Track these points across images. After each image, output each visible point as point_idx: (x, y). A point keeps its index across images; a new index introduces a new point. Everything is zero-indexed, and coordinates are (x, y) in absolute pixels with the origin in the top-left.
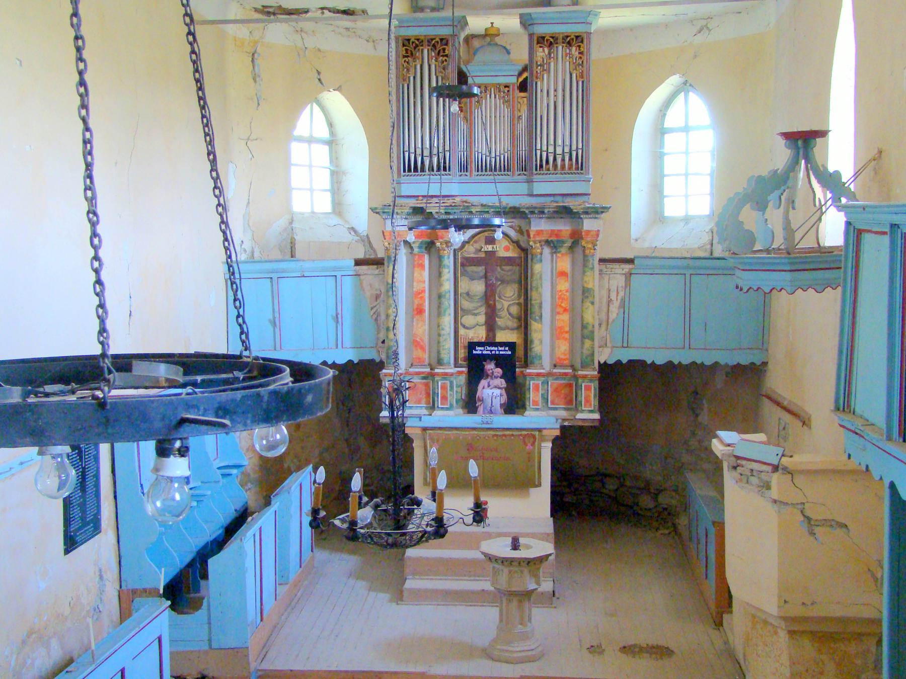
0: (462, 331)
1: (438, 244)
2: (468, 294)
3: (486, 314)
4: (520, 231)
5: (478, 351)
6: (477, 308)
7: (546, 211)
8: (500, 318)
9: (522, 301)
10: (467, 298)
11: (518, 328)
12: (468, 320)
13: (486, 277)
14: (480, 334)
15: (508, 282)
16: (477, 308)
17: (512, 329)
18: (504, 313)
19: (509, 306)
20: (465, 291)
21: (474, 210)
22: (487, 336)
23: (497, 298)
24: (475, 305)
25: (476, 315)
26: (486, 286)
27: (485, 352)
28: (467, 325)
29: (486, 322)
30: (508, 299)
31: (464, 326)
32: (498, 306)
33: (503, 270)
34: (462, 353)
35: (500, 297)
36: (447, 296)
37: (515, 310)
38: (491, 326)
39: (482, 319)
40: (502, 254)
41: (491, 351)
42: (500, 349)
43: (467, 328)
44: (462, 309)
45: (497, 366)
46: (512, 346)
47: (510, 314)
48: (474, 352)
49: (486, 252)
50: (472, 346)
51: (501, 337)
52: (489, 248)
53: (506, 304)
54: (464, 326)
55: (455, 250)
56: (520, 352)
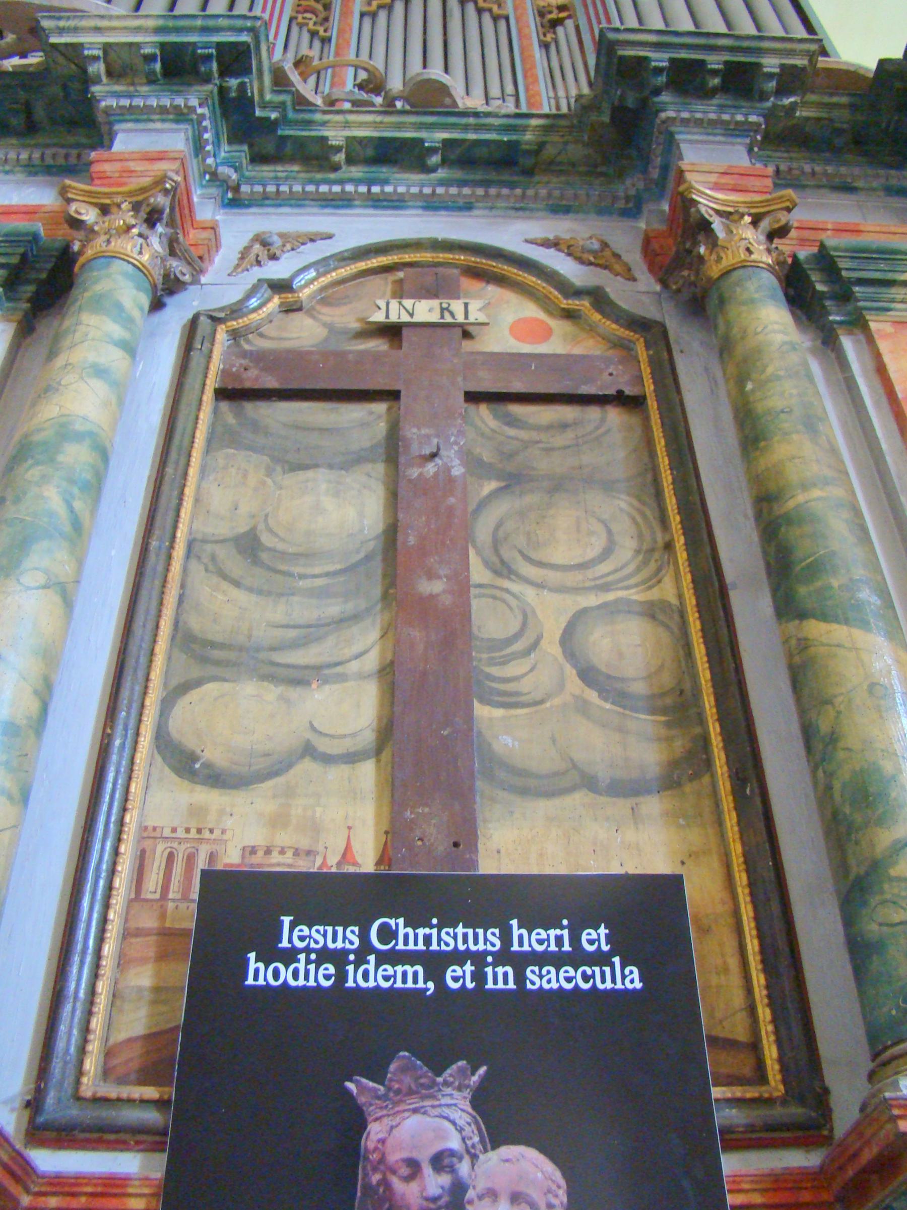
0: (159, 802)
1: (90, 215)
2: (249, 545)
3: (388, 674)
4: (601, 257)
5: (302, 960)
6: (312, 633)
7: (771, 64)
8: (510, 701)
9: (677, 587)
10: (235, 564)
11: (670, 781)
12: (233, 716)
13: (393, 449)
14: (341, 823)
15: (558, 486)
16: (312, 633)
17: (627, 788)
18: (543, 671)
19: (581, 615)
20: (223, 530)
21: (336, 136)
22: (395, 835)
23: (478, 573)
24: (303, 611)
25: (300, 678)
26: (393, 498)
27: (371, 977)
28: (213, 754)
29: (387, 731)
30: (569, 592)
31: (185, 763)
32: (489, 621)
33: (512, 422)
34: (131, 1000)
35: (503, 569)
36: (76, 456)
37: (630, 647)
38: (427, 740)
39: (350, 709)
40: (499, 339)
41: (435, 963)
42: (526, 940)
43: (216, 779)
44: (184, 638)
45: (500, 1122)
46: (645, 914)
47: (588, 675)
48: (259, 973)
49: (392, 332)
50: (239, 909)
51: (515, 842)
52: (425, 311)
53: (552, 613)
54: (185, 763)
55: (194, 323)
56: (726, 984)
